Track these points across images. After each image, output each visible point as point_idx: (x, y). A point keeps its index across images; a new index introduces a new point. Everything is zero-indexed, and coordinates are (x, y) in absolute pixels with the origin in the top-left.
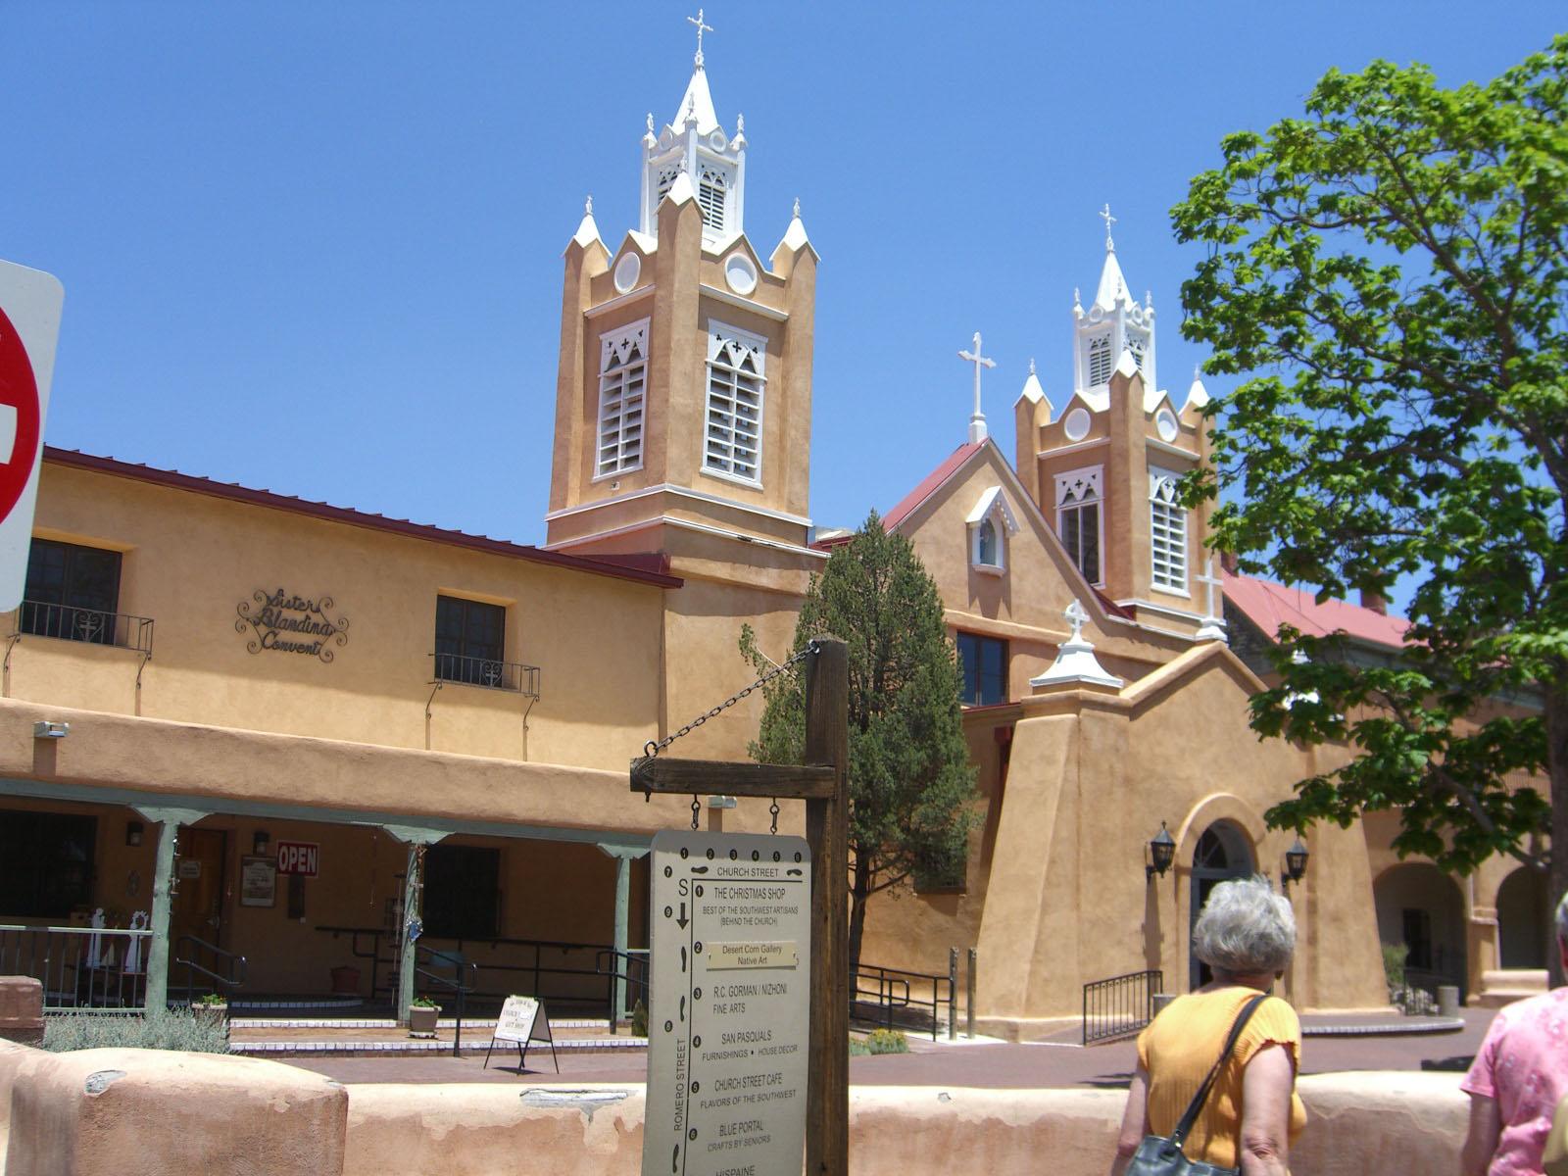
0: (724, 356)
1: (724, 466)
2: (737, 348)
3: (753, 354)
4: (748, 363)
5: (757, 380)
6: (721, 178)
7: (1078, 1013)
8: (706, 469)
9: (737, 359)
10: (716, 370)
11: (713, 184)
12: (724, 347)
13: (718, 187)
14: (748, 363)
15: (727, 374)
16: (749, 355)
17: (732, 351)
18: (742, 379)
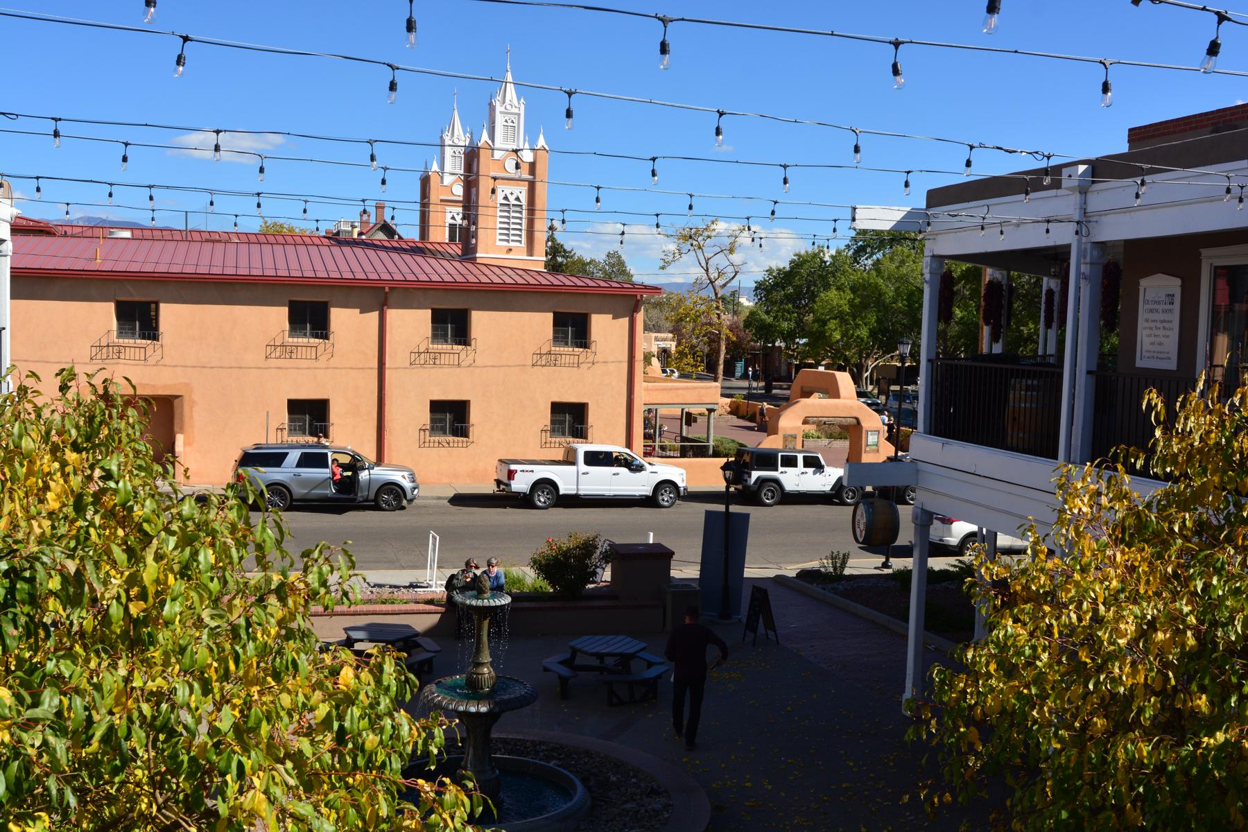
0: (506, 198)
2: (512, 194)
3: (519, 195)
10: (501, 204)
13: (512, 124)
14: (518, 199)
17: (509, 196)
18: (513, 205)
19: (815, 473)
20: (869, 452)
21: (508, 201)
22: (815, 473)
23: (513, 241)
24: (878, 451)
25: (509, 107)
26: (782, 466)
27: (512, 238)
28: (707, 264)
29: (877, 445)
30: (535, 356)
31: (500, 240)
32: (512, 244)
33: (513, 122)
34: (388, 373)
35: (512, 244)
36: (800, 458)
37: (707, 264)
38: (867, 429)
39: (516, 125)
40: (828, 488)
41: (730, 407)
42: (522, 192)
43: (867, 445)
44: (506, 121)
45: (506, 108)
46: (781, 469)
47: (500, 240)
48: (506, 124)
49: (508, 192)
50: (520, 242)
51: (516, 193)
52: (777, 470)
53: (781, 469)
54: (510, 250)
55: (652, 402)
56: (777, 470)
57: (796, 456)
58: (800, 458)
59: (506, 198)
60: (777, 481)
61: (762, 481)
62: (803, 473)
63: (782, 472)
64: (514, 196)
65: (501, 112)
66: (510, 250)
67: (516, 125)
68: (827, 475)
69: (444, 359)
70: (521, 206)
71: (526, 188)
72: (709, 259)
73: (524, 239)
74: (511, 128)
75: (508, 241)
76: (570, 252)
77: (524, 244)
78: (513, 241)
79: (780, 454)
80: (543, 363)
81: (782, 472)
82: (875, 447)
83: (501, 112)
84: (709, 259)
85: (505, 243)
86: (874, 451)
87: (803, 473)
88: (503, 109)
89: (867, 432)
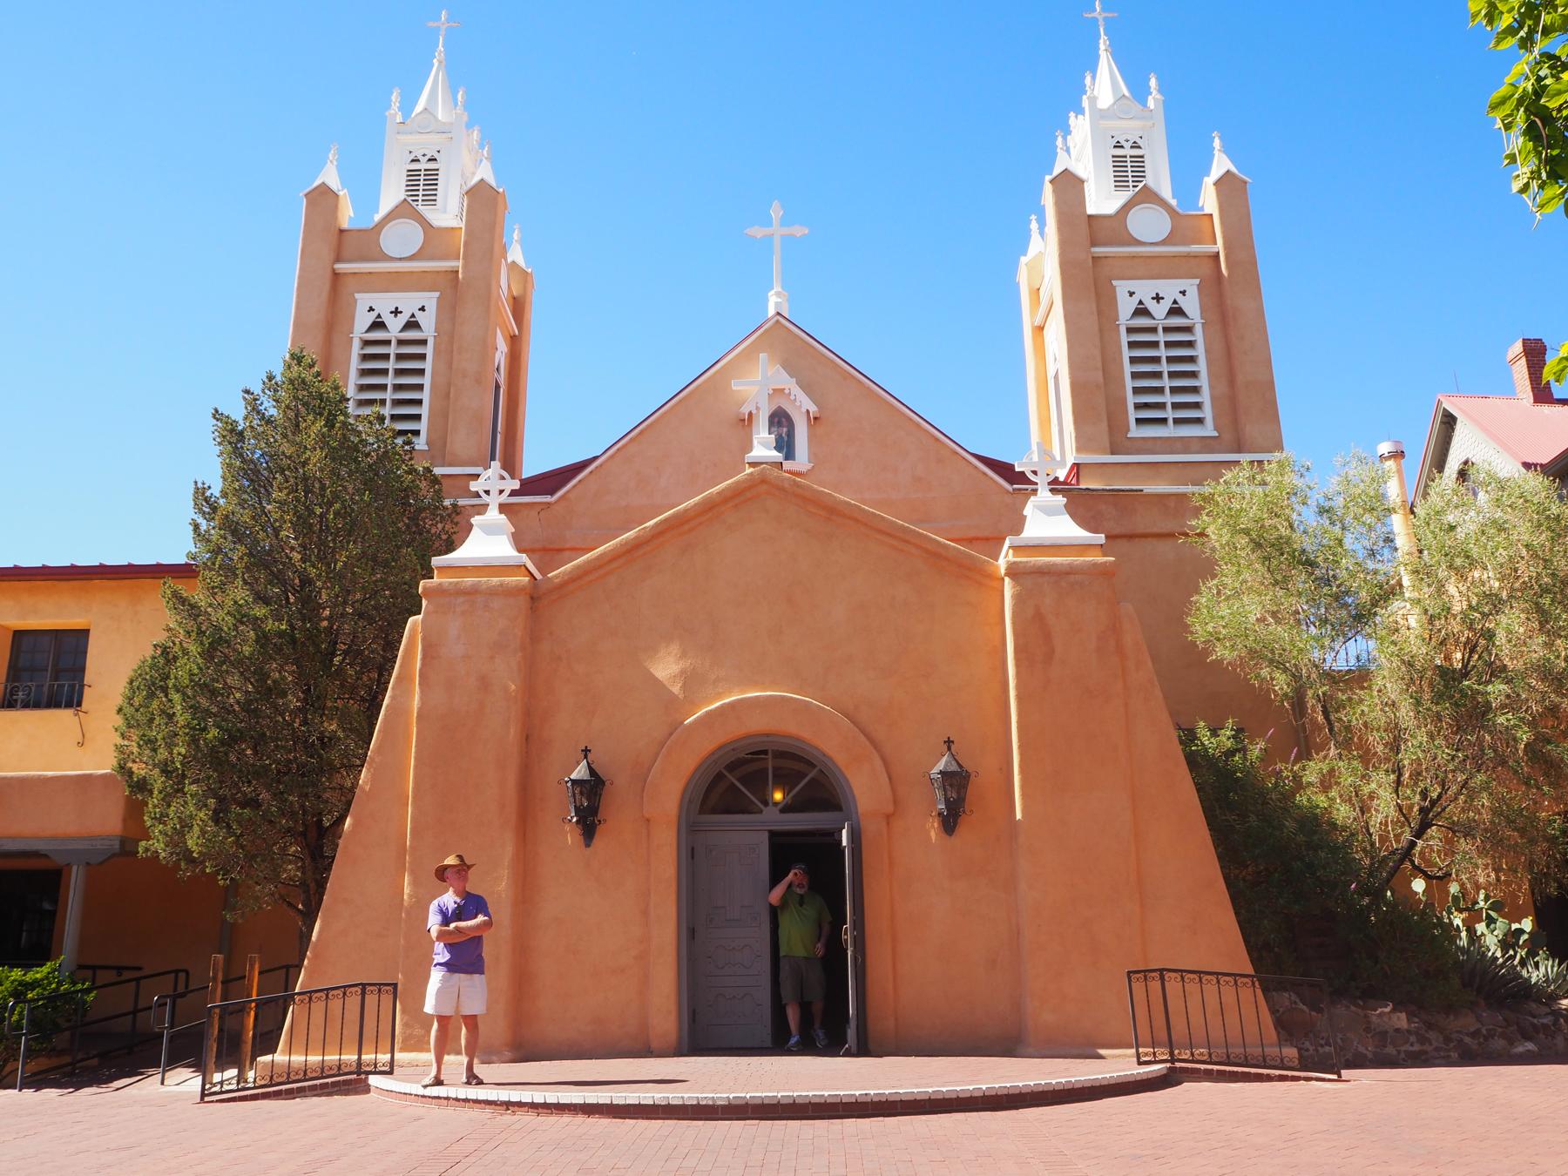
1: (1164, 421)
2: (1158, 298)
3: (1180, 298)
4: (1176, 311)
5: (1194, 324)
6: (1139, 141)
7: (301, 1055)
8: (1135, 432)
9: (1159, 311)
10: (1130, 330)
11: (1128, 151)
12: (1141, 302)
14: (1176, 311)
15: (1153, 330)
16: (1175, 302)
17: (1151, 305)
18: (1167, 330)
31: (1139, 421)
47: (1139, 421)
59: (1141, 311)
64: (1166, 305)
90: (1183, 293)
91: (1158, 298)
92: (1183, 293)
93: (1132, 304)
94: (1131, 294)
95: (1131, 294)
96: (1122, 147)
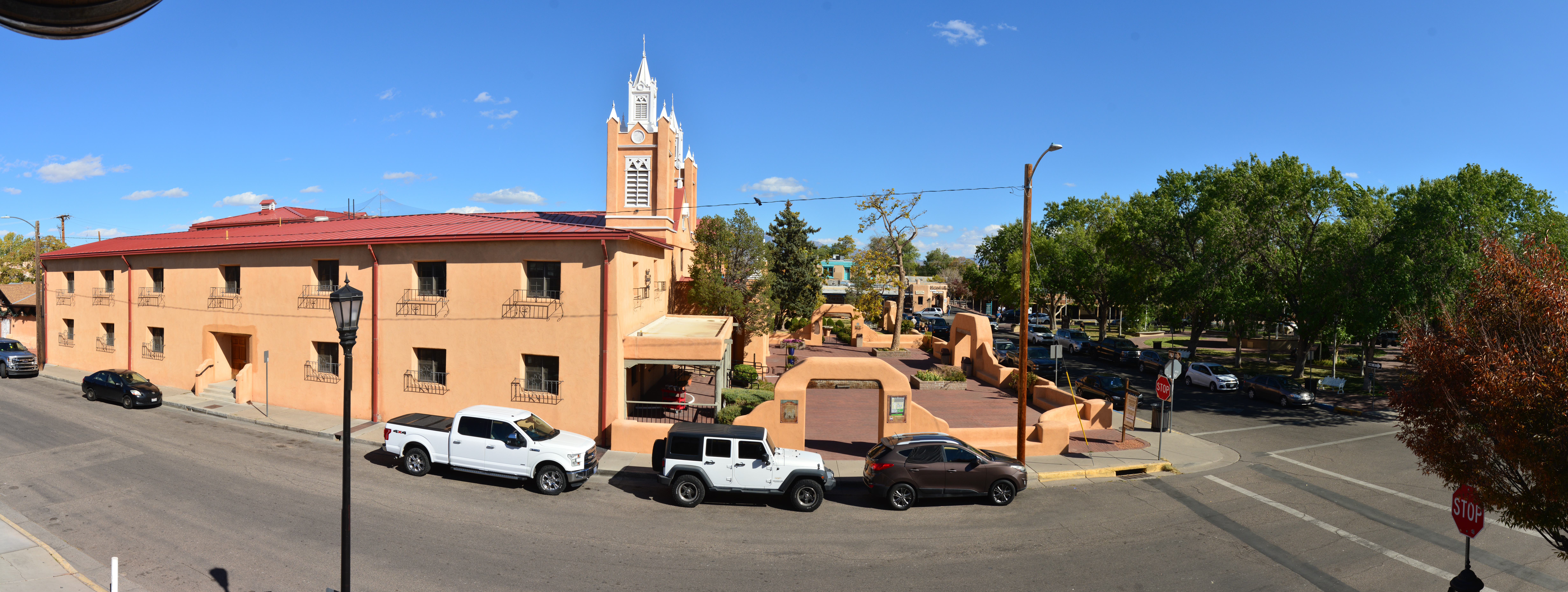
0: (633, 166)
3: (645, 162)
10: (629, 172)
13: (644, 102)
14: (643, 166)
15: (635, 172)
17: (636, 164)
18: (640, 172)
19: (755, 466)
20: (893, 421)
21: (635, 168)
22: (755, 466)
23: (639, 203)
24: (905, 421)
25: (640, 88)
26: (708, 454)
27: (639, 200)
28: (890, 226)
29: (903, 413)
30: (505, 307)
31: (628, 203)
32: (639, 206)
33: (645, 101)
34: (379, 323)
35: (639, 206)
36: (735, 443)
37: (890, 226)
38: (890, 394)
39: (647, 102)
40: (776, 486)
41: (923, 341)
42: (646, 159)
43: (890, 414)
44: (639, 100)
45: (637, 89)
46: (705, 458)
47: (628, 203)
48: (638, 102)
49: (634, 160)
50: (646, 203)
51: (642, 160)
52: (700, 459)
53: (705, 458)
54: (637, 211)
55: (641, 357)
56: (700, 459)
57: (729, 442)
58: (735, 443)
59: (633, 166)
60: (698, 474)
61: (678, 472)
62: (737, 465)
63: (707, 463)
64: (641, 164)
65: (633, 93)
66: (637, 211)
67: (647, 102)
68: (775, 468)
69: (424, 309)
70: (647, 172)
71: (651, 156)
72: (891, 223)
73: (649, 201)
74: (643, 107)
75: (635, 203)
76: (802, 222)
77: (649, 206)
78: (639, 203)
79: (706, 438)
80: (513, 315)
81: (707, 463)
82: (900, 416)
83: (633, 93)
84: (891, 223)
85: (633, 206)
86: (899, 421)
87: (737, 465)
88: (635, 90)
89: (890, 397)
90: (646, 160)
91: (638, 162)
92: (646, 160)
93: (630, 164)
94: (630, 160)
95: (630, 160)
96: (639, 101)
